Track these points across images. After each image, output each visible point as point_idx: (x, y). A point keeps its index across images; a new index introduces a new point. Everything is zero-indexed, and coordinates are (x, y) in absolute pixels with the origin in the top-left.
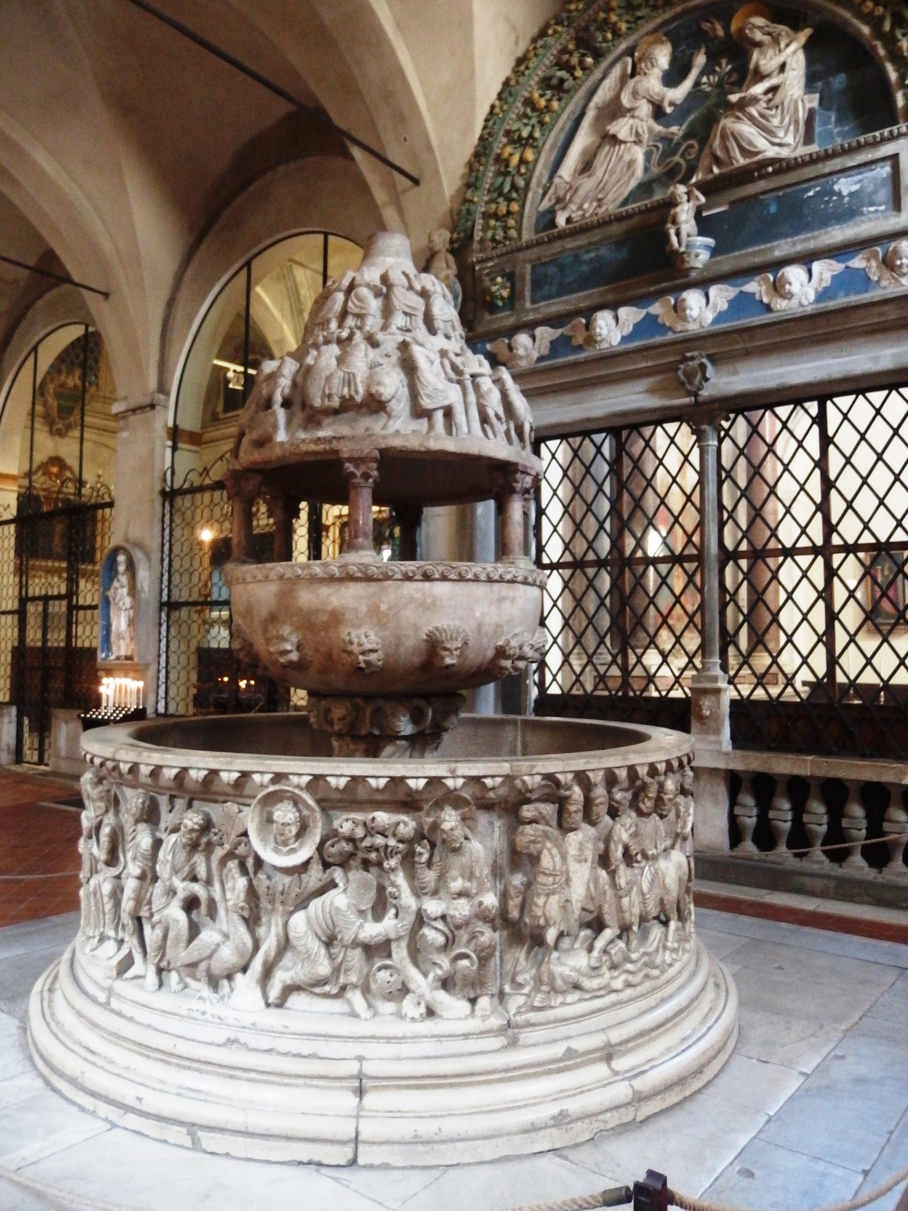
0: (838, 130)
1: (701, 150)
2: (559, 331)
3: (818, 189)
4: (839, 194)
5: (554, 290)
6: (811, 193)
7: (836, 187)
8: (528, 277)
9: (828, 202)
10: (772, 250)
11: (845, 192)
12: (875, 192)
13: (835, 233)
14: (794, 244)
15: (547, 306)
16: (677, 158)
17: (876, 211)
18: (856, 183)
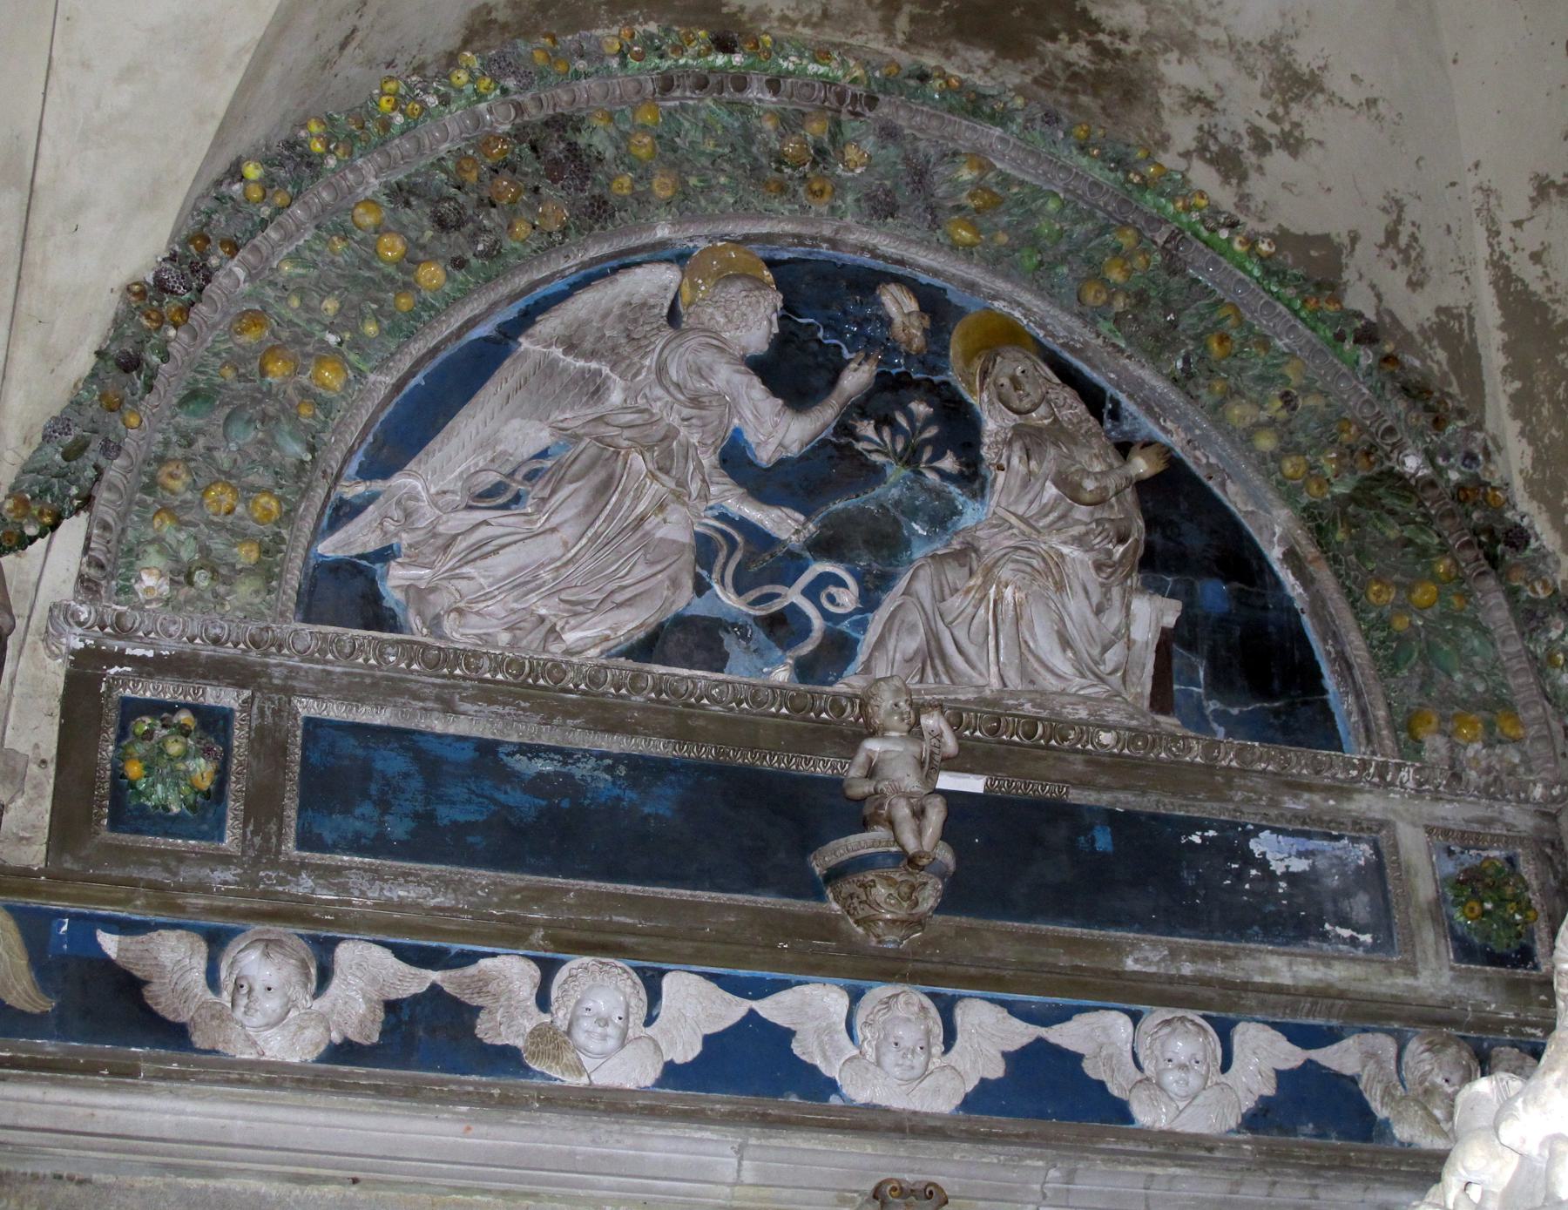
0: (1212, 706)
1: (869, 602)
2: (435, 976)
3: (1211, 833)
4: (1263, 864)
5: (398, 828)
6: (1196, 839)
7: (1255, 846)
8: (296, 754)
9: (1240, 876)
10: (1119, 949)
11: (1278, 867)
12: (1346, 893)
13: (1274, 962)
14: (1174, 954)
15: (376, 875)
16: (793, 595)
17: (1353, 941)
18: (1300, 855)
